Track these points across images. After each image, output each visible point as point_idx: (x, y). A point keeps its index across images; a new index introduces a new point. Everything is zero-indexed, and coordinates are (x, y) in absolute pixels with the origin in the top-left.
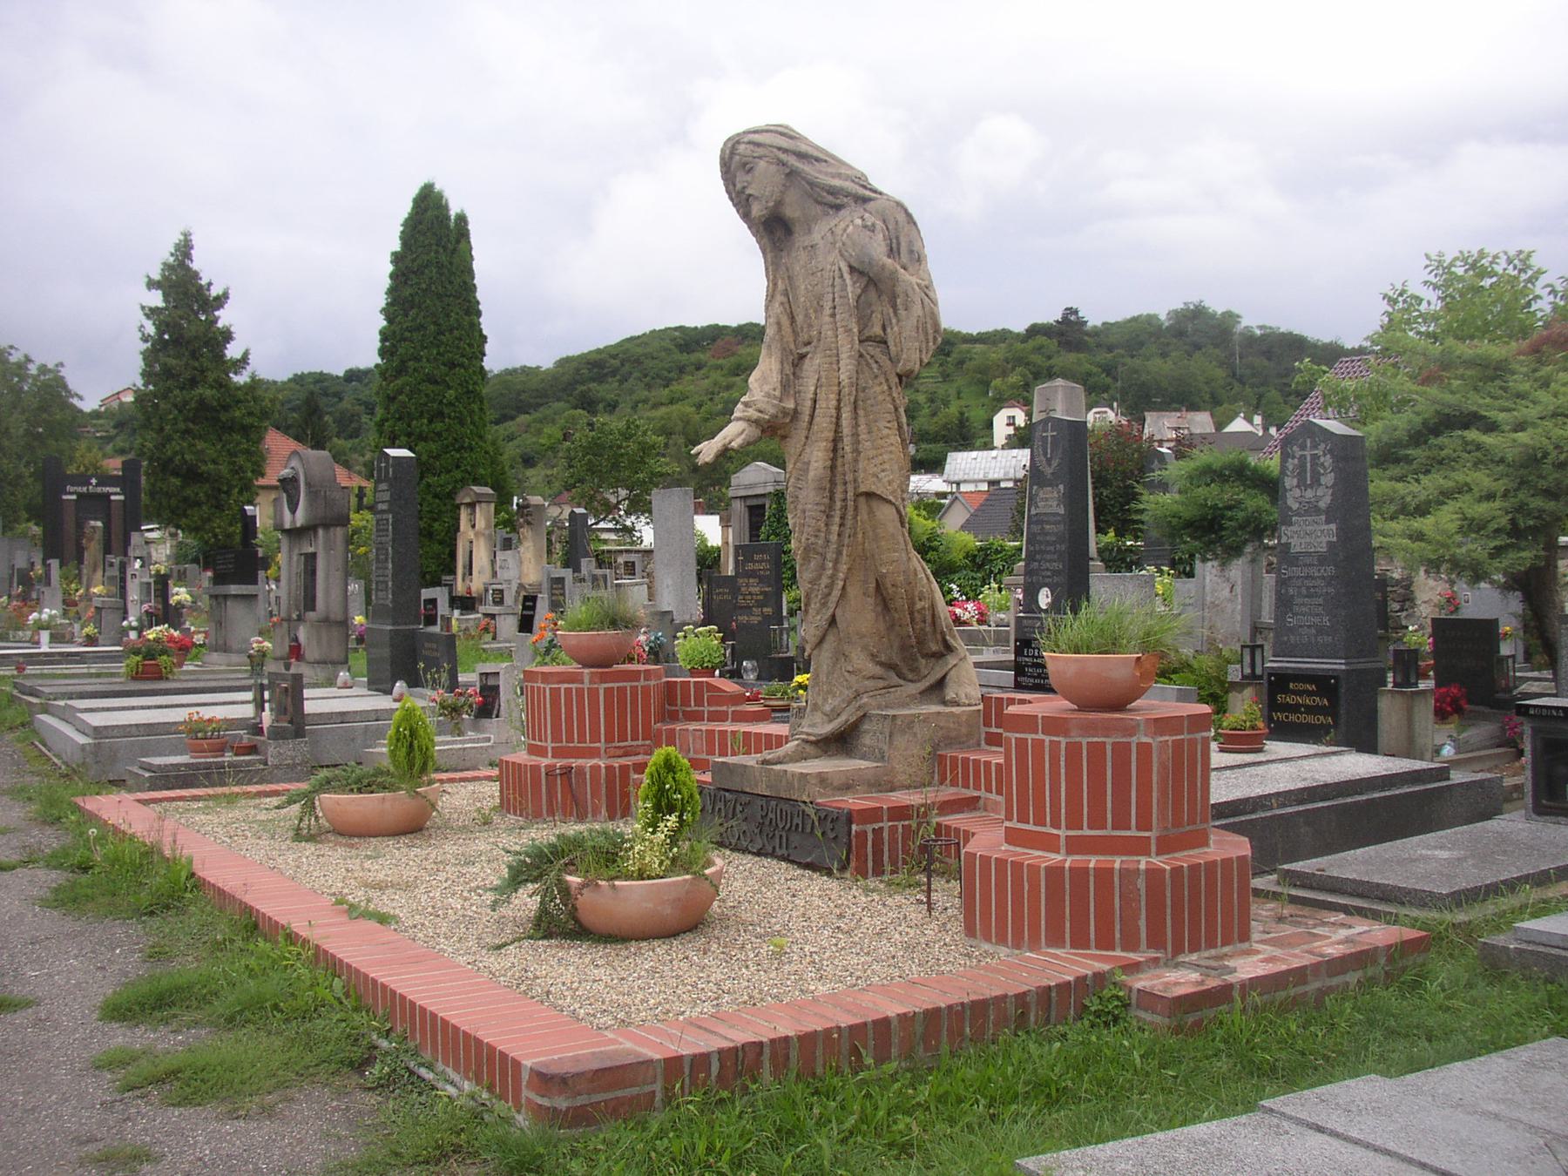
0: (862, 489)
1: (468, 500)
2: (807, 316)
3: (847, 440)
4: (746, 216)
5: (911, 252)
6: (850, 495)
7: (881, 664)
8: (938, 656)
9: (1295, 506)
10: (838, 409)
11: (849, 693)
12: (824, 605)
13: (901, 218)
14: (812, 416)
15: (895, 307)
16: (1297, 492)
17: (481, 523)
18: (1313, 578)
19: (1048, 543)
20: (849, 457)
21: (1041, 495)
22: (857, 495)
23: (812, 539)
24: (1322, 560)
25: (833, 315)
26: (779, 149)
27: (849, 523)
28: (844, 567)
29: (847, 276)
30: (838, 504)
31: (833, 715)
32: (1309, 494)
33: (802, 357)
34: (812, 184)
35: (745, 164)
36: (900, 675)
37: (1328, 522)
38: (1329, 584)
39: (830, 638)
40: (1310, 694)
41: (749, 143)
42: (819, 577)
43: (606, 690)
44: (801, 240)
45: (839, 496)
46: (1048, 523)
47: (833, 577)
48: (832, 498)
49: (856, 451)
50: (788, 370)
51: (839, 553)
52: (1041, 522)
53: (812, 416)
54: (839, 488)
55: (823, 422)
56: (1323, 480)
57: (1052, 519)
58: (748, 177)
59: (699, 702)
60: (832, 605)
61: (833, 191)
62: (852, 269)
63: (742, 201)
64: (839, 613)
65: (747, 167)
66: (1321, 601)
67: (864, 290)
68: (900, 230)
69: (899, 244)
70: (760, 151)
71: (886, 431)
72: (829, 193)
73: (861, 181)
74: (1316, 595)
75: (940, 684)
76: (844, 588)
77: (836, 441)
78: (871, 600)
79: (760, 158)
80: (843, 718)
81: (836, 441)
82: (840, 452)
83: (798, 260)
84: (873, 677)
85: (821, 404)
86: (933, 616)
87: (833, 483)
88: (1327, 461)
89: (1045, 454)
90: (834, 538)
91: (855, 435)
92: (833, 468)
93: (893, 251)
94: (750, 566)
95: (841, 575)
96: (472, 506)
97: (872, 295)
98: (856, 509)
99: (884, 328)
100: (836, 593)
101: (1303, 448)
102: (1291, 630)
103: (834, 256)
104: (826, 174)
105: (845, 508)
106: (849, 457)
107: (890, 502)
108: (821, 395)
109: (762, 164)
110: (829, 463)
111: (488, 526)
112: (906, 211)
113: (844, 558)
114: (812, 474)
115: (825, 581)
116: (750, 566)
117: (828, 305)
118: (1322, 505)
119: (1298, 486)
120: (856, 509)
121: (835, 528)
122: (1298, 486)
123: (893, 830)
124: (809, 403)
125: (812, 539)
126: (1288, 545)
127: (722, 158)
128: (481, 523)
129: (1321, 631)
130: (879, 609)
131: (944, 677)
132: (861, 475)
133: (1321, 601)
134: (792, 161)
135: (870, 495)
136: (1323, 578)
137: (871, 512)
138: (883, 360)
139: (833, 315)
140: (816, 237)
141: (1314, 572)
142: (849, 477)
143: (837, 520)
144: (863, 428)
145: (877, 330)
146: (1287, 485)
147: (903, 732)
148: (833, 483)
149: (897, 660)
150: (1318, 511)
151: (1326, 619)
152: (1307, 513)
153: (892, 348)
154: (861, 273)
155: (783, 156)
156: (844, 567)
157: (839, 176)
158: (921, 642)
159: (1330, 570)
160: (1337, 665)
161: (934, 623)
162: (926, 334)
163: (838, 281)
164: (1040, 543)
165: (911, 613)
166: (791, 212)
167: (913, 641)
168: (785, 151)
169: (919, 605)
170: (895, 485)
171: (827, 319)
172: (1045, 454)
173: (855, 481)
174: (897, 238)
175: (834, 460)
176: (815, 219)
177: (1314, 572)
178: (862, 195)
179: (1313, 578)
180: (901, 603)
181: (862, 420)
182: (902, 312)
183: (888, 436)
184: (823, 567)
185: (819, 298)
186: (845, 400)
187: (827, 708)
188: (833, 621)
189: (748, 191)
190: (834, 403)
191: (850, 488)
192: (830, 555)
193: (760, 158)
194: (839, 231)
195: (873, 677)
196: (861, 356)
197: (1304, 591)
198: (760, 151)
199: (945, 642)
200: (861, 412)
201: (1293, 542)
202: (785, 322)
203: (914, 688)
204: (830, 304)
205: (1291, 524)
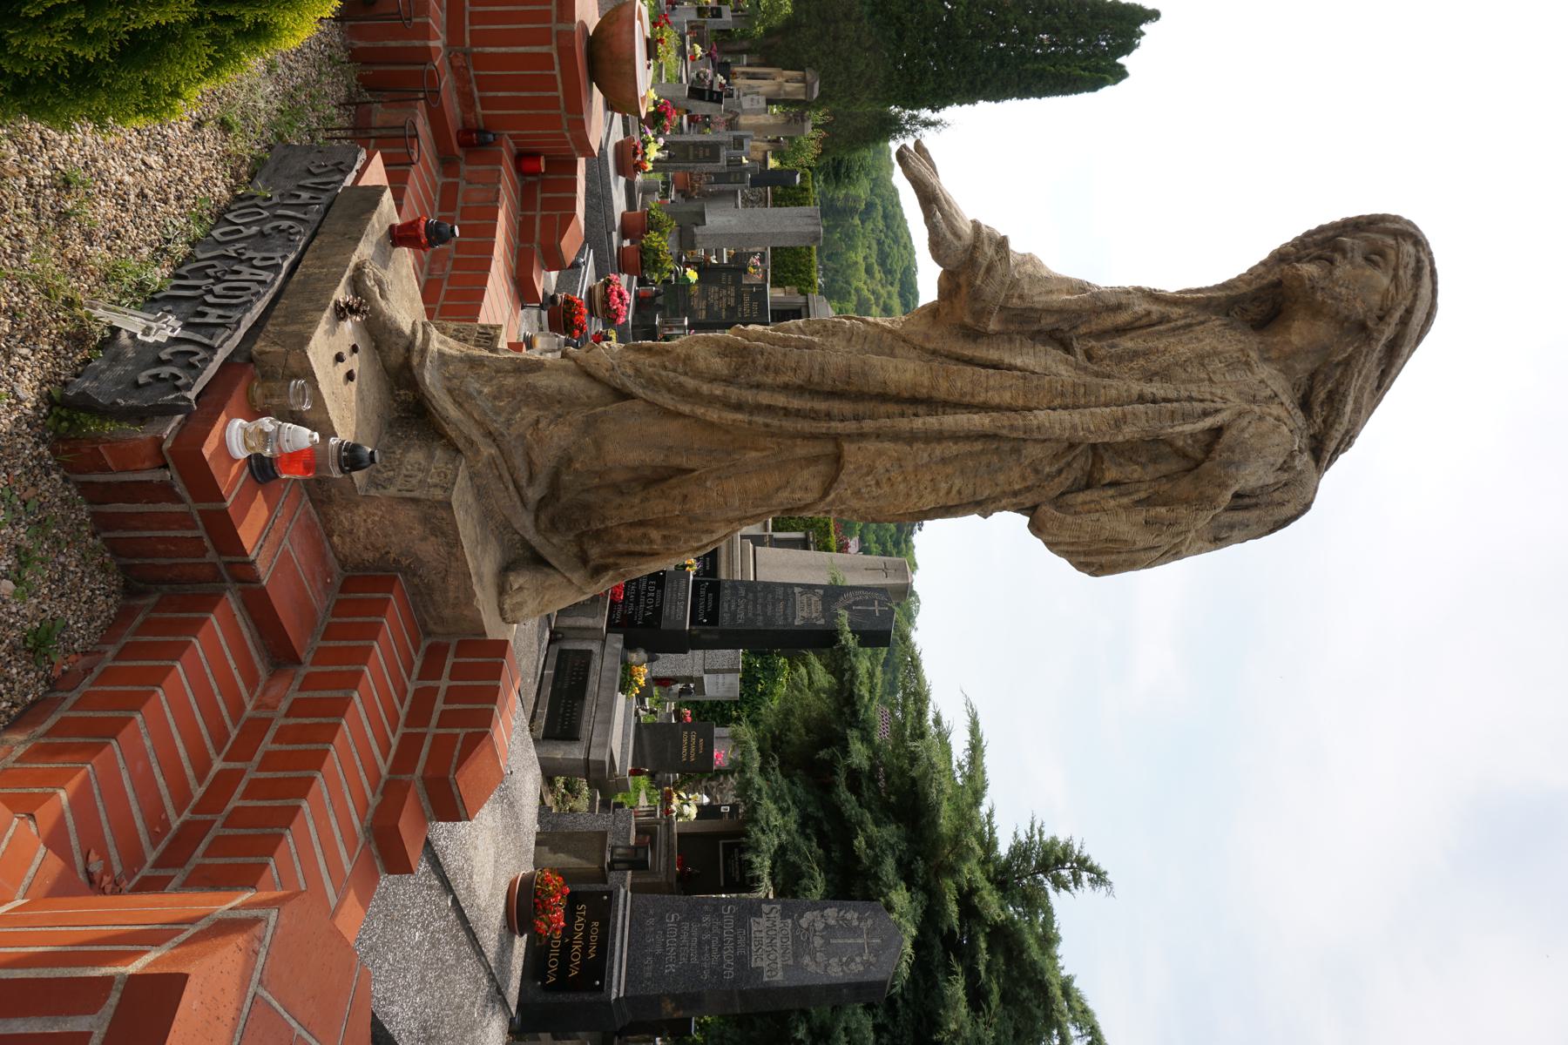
0: (849, 448)
1: (809, 77)
2: (1135, 354)
3: (932, 422)
4: (1281, 257)
5: (1232, 527)
6: (837, 426)
7: (556, 475)
8: (584, 559)
9: (804, 923)
10: (984, 408)
11: (497, 425)
12: (651, 383)
13: (1288, 510)
14: (970, 362)
15: (1148, 502)
16: (820, 925)
17: (789, 87)
18: (720, 949)
19: (765, 606)
20: (903, 424)
21: (814, 599)
22: (836, 438)
23: (761, 361)
24: (742, 961)
25: (1141, 399)
26: (1409, 312)
27: (789, 425)
28: (713, 415)
29: (1208, 422)
30: (822, 406)
31: (460, 397)
32: (818, 942)
33: (1067, 348)
34: (1347, 363)
35: (1382, 254)
36: (542, 503)
37: (786, 968)
38: (713, 972)
39: (595, 391)
40: (585, 949)
41: (1419, 261)
42: (698, 375)
43: (550, 55)
44: (1252, 343)
45: (836, 406)
46: (786, 606)
47: (695, 396)
48: (832, 394)
49: (912, 438)
50: (1047, 322)
51: (738, 407)
52: (786, 600)
53: (970, 362)
54: (847, 407)
55: (963, 380)
56: (834, 961)
57: (789, 612)
58: (1359, 260)
59: (547, 204)
60: (650, 396)
61: (1334, 400)
62: (1217, 432)
63: (1325, 244)
64: (638, 406)
65: (1375, 256)
66: (694, 960)
67: (1182, 454)
68: (1273, 506)
69: (1247, 508)
70: (1406, 276)
71: (944, 486)
72: (1331, 395)
73: (1347, 441)
74: (701, 954)
75: (537, 561)
76: (679, 415)
77: (931, 404)
78: (659, 459)
79: (1395, 278)
80: (452, 412)
81: (931, 404)
82: (910, 410)
83: (1216, 338)
84: (530, 463)
85: (994, 378)
86: (642, 554)
87: (861, 396)
88: (857, 967)
89: (856, 603)
90: (764, 398)
91: (940, 437)
92: (883, 397)
93: (1242, 500)
94: (747, 299)
95: (700, 411)
96: (803, 80)
97: (1173, 465)
98: (814, 437)
99: (1112, 484)
100: (666, 400)
101: (871, 931)
102: (662, 918)
103: (1236, 403)
104: (1362, 388)
105: (814, 415)
106: (903, 424)
107: (826, 493)
108: (1008, 378)
109: (1385, 281)
110: (892, 389)
111: (786, 93)
112: (1295, 518)
113: (730, 416)
114: (875, 360)
115: (691, 383)
116: (747, 299)
117: (1155, 388)
118: (807, 960)
119: (827, 926)
120: (814, 437)
121: (780, 400)
122: (827, 926)
123: (184, 520)
124: (993, 355)
125: (761, 361)
126: (758, 913)
127: (1384, 218)
128: (789, 87)
129: (659, 960)
130: (648, 473)
131: (548, 565)
132: (872, 446)
133: (694, 960)
134: (1389, 332)
135: (837, 460)
136: (721, 962)
137: (813, 460)
138: (1066, 480)
139: (1141, 399)
140: (1265, 371)
141: (729, 946)
142: (868, 425)
143: (795, 403)
144: (953, 449)
145: (1112, 474)
146: (828, 911)
147: (425, 520)
148: (861, 396)
149: (565, 498)
150: (796, 956)
151: (672, 968)
152: (796, 940)
153: (1081, 497)
154: (1208, 449)
155: (1397, 315)
156: (713, 415)
157: (1357, 410)
158: (597, 536)
159: (730, 974)
160: (617, 989)
161: (630, 554)
162: (1099, 552)
163: (1198, 406)
164: (765, 598)
165: (642, 523)
166: (1300, 333)
167: (597, 525)
168: (1404, 322)
169: (655, 534)
170: (855, 504)
171: (1136, 388)
172: (856, 603)
173: (862, 436)
174: (1256, 505)
175: (898, 399)
176: (1287, 371)
177: (729, 946)
178: (1325, 445)
179: (720, 949)
180: (657, 507)
181: (964, 447)
182: (1140, 516)
183: (935, 490)
184: (714, 379)
185: (1164, 375)
186: (1004, 419)
187: (473, 385)
188: (622, 395)
189: (1338, 257)
190: (995, 398)
191: (851, 426)
192: (734, 393)
193: (1395, 278)
194: (1275, 410)
195: (530, 463)
196: (1072, 446)
197: (707, 937)
198: (1406, 276)
199: (606, 568)
200: (978, 446)
201: (763, 920)
202: (1123, 318)
203: (525, 523)
204: (1161, 393)
205: (784, 916)
